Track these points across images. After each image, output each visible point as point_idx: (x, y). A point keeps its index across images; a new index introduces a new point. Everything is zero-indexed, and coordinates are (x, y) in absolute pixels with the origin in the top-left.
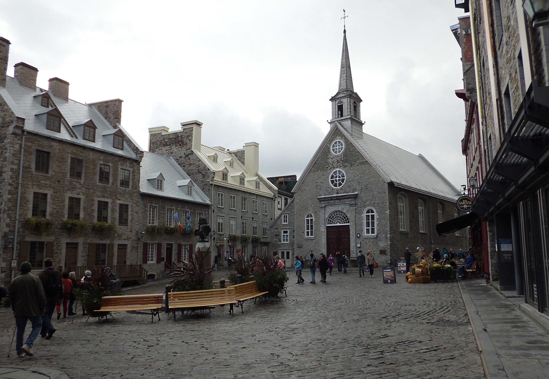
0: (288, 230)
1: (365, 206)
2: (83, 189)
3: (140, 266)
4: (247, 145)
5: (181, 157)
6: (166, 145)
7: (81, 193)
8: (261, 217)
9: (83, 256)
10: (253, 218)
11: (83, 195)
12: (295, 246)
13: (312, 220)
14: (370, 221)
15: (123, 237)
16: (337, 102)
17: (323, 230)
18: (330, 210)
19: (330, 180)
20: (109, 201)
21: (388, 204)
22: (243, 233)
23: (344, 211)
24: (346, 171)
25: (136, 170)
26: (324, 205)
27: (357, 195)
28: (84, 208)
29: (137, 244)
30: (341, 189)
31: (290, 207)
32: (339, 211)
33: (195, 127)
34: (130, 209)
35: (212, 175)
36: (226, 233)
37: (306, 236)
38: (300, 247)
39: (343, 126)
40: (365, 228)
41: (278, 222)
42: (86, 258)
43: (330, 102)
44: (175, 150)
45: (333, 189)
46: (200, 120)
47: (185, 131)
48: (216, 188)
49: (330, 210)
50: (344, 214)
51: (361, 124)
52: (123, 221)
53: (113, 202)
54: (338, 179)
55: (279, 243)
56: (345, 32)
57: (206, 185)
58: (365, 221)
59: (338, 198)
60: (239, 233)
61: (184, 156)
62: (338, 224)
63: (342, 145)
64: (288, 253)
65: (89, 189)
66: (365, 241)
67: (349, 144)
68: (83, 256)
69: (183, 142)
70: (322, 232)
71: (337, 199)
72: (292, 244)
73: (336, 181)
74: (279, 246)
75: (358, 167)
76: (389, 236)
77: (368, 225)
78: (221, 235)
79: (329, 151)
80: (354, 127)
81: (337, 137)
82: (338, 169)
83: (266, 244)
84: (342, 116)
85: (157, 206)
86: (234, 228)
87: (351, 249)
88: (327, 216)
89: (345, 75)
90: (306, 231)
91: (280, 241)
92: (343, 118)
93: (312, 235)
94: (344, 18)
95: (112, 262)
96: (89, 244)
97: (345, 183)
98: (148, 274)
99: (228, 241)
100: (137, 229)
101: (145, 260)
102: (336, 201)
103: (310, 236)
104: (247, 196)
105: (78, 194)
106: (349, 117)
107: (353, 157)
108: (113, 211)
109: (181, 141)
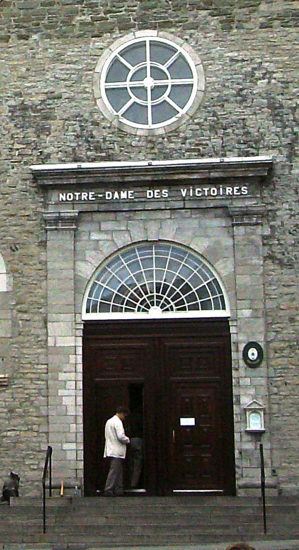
17: (66, 338)
24: (197, 48)
26: (69, 212)
30: (174, 133)
45: (120, 131)
54: (149, 82)
62: (155, 313)
71: (152, 185)
75: (263, 34)
88: (86, 269)
102: (150, 193)
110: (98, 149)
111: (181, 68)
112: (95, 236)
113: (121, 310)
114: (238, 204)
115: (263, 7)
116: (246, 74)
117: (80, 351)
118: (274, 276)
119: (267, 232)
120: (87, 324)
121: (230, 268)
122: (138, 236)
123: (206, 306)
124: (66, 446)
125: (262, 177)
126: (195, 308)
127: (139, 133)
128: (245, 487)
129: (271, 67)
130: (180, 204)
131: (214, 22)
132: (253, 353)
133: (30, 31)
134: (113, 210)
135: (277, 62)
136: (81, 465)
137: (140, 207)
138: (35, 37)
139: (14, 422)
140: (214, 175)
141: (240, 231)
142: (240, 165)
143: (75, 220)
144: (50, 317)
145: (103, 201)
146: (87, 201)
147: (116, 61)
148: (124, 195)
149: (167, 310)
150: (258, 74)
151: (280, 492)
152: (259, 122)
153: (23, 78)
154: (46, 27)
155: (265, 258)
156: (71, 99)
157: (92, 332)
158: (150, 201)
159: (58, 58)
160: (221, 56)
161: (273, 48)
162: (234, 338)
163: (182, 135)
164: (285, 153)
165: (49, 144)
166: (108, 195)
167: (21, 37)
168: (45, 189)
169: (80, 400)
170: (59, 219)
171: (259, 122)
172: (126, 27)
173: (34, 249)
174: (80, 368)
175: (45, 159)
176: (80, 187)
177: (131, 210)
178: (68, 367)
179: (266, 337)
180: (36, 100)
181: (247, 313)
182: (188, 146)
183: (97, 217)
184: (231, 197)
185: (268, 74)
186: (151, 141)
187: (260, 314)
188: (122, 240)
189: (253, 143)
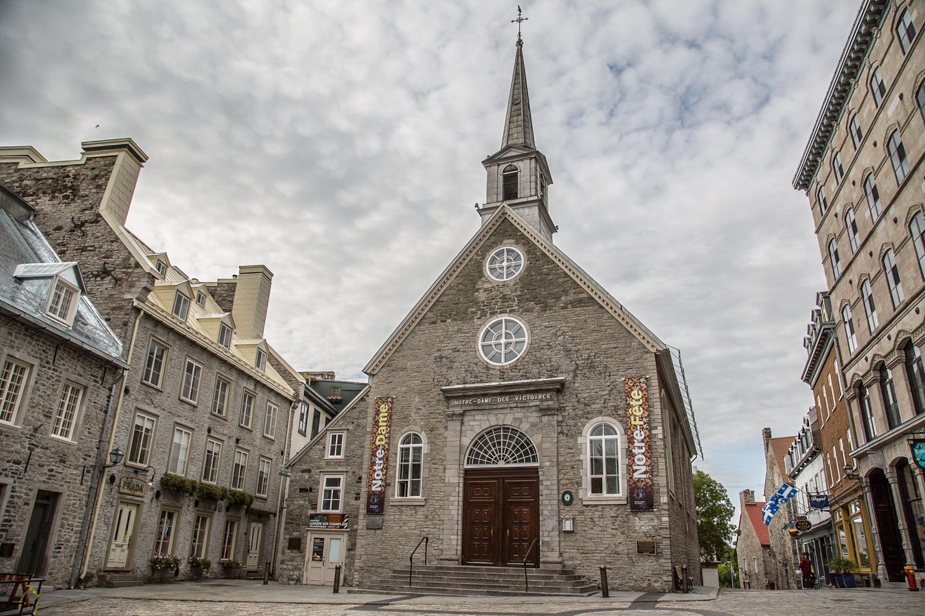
0: (342, 478)
1: (588, 416)
4: (246, 271)
5: (59, 228)
8: (258, 442)
16: (502, 167)
17: (454, 477)
18: (478, 424)
19: (480, 343)
22: (206, 477)
23: (524, 427)
24: (529, 322)
26: (459, 410)
27: (562, 383)
30: (514, 367)
31: (355, 413)
32: (506, 429)
33: (122, 156)
35: (144, 283)
36: (157, 467)
37: (397, 497)
40: (587, 477)
45: (488, 368)
46: (141, 144)
47: (91, 164)
48: (149, 326)
49: (478, 424)
50: (522, 435)
51: (553, 229)
54: (503, 341)
55: (311, 512)
56: (520, 43)
57: (120, 308)
58: (586, 457)
59: (506, 391)
61: (68, 225)
62: (502, 464)
66: (588, 514)
69: (75, 190)
70: (450, 485)
71: (500, 394)
75: (564, 312)
78: (136, 471)
81: (505, 242)
82: (504, 317)
86: (182, 456)
87: (544, 537)
88: (467, 441)
89: (521, 118)
90: (397, 480)
91: (314, 507)
93: (415, 492)
94: (520, 20)
97: (528, 352)
99: (158, 495)
102: (499, 399)
103: (409, 497)
104: (233, 376)
106: (535, 198)
107: (551, 286)
109: (70, 188)
110: (476, 377)
111: (519, 332)
112: (471, 423)
113: (482, 462)
114: (545, 403)
115: (563, 298)
117: (461, 485)
118: (563, 443)
119: (560, 418)
120: (466, 471)
121: (540, 439)
122: (494, 422)
123: (528, 460)
124: (452, 537)
125: (560, 389)
126: (521, 461)
128: (544, 562)
129: (566, 329)
130: (515, 405)
131: (537, 308)
133: (446, 317)
134: (481, 409)
136: (460, 548)
137: (494, 407)
138: (449, 321)
139: (428, 523)
140: (532, 388)
141: (545, 419)
142: (545, 382)
143: (462, 415)
144: (447, 467)
145: (475, 404)
146: (468, 405)
147: (488, 332)
148: (486, 401)
151: (564, 566)
152: (558, 358)
153: (442, 342)
155: (559, 433)
156: (464, 352)
158: (499, 404)
159: (459, 331)
160: (540, 325)
161: (566, 318)
162: (541, 478)
165: (452, 375)
166: (479, 401)
167: (442, 321)
168: (448, 399)
169: (460, 512)
170: (453, 415)
171: (558, 358)
172: (493, 314)
173: (442, 430)
174: (461, 494)
176: (464, 397)
177: (489, 409)
183: (473, 413)
184: (542, 400)
186: (503, 373)
187: (555, 464)
188: (486, 425)
189: (555, 370)
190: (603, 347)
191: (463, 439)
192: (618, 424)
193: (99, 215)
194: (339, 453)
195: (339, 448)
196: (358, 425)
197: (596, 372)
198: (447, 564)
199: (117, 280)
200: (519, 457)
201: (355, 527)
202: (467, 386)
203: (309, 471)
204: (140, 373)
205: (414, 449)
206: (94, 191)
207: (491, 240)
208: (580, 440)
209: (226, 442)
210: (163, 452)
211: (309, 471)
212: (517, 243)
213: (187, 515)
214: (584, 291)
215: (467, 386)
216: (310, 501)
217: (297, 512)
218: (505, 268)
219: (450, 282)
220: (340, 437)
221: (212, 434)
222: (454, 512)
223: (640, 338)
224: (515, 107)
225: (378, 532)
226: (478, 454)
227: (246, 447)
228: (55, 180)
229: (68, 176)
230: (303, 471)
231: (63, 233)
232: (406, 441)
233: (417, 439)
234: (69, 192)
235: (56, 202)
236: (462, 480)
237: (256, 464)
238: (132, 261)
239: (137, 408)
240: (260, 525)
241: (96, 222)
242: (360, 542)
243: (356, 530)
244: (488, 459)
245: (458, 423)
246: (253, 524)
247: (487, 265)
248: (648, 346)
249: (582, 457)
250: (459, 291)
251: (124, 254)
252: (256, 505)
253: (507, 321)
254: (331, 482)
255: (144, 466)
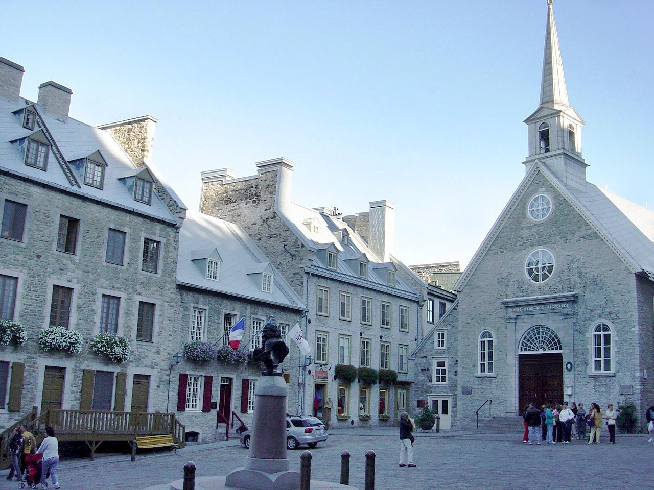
0: (446, 361)
2: (77, 271)
3: (173, 416)
6: (229, 202)
7: (74, 280)
9: (72, 392)
10: (381, 337)
11: (78, 282)
12: (459, 391)
13: (490, 342)
14: (602, 346)
15: (147, 361)
20: (123, 295)
21: (636, 315)
23: (553, 327)
25: (172, 242)
26: (513, 315)
27: (576, 297)
28: (79, 307)
29: (169, 375)
30: (547, 284)
31: (450, 318)
34: (157, 313)
38: (467, 392)
39: (549, 168)
41: (428, 346)
42: (78, 395)
43: (526, 126)
44: (246, 211)
49: (525, 325)
50: (553, 332)
52: (145, 332)
53: (130, 298)
55: (429, 384)
57: (298, 273)
59: (541, 303)
60: (356, 363)
61: (260, 222)
62: (541, 352)
63: (548, 203)
64: (445, 403)
65: (88, 272)
67: (561, 202)
68: (72, 392)
72: (453, 386)
73: (537, 269)
74: (429, 389)
76: (638, 374)
77: (598, 353)
79: (524, 214)
80: (570, 170)
83: (405, 385)
84: (547, 150)
85: (207, 308)
88: (519, 336)
91: (431, 381)
92: (548, 154)
95: (123, 406)
96: (84, 370)
98: (186, 431)
100: (169, 350)
101: (181, 406)
105: (70, 281)
106: (561, 151)
108: (128, 314)
109: (256, 195)
113: (529, 350)
115: (577, 233)
116: (571, 261)
117: (517, 365)
119: (575, 321)
120: (520, 356)
123: (557, 348)
125: (574, 300)
126: (553, 349)
127: (536, 285)
129: (578, 257)
131: (561, 241)
132: (569, 366)
135: (581, 255)
138: (505, 252)
148: (530, 309)
149: (545, 350)
150: (575, 260)
152: (575, 279)
154: (509, 248)
155: (574, 331)
157: (521, 358)
159: (512, 259)
163: (549, 285)
164: (583, 290)
171: (575, 279)
172: (533, 245)
173: (504, 329)
174: (517, 371)
175: (507, 296)
178: (512, 371)
179: (574, 360)
180: (504, 275)
181: (568, 351)
182: (551, 289)
185: (578, 260)
187: (572, 351)
190: (603, 270)
191: (517, 335)
192: (611, 324)
193: (275, 213)
194: (443, 346)
195: (443, 341)
196: (453, 326)
197: (598, 288)
198: (509, 415)
199: (293, 256)
200: (551, 346)
201: (456, 393)
202: (518, 299)
203: (425, 357)
204: (315, 309)
205: (489, 341)
206: (269, 196)
207: (530, 189)
208: (587, 335)
209: (373, 340)
210: (335, 352)
211: (425, 357)
212: (547, 191)
213: (355, 387)
214: (591, 228)
215: (518, 299)
216: (428, 377)
217: (421, 384)
218: (541, 209)
219: (504, 222)
220: (443, 334)
221: (363, 336)
222: (513, 383)
223: (625, 262)
224: (547, 67)
225: (469, 395)
226: (527, 344)
227: (388, 340)
228: (246, 190)
229: (252, 187)
230: (422, 358)
231: (257, 226)
232: (483, 336)
233: (490, 336)
234: (255, 198)
235: (248, 205)
236: (517, 362)
237: (396, 350)
238: (299, 243)
239: (316, 330)
240: (405, 391)
241: (274, 217)
242: (459, 402)
243: (456, 395)
244: (533, 348)
245: (513, 324)
246: (399, 391)
247: (529, 210)
248: (631, 268)
249: (588, 347)
250: (511, 229)
251: (294, 238)
252: (400, 378)
253: (541, 250)
254: (441, 364)
255: (324, 362)
